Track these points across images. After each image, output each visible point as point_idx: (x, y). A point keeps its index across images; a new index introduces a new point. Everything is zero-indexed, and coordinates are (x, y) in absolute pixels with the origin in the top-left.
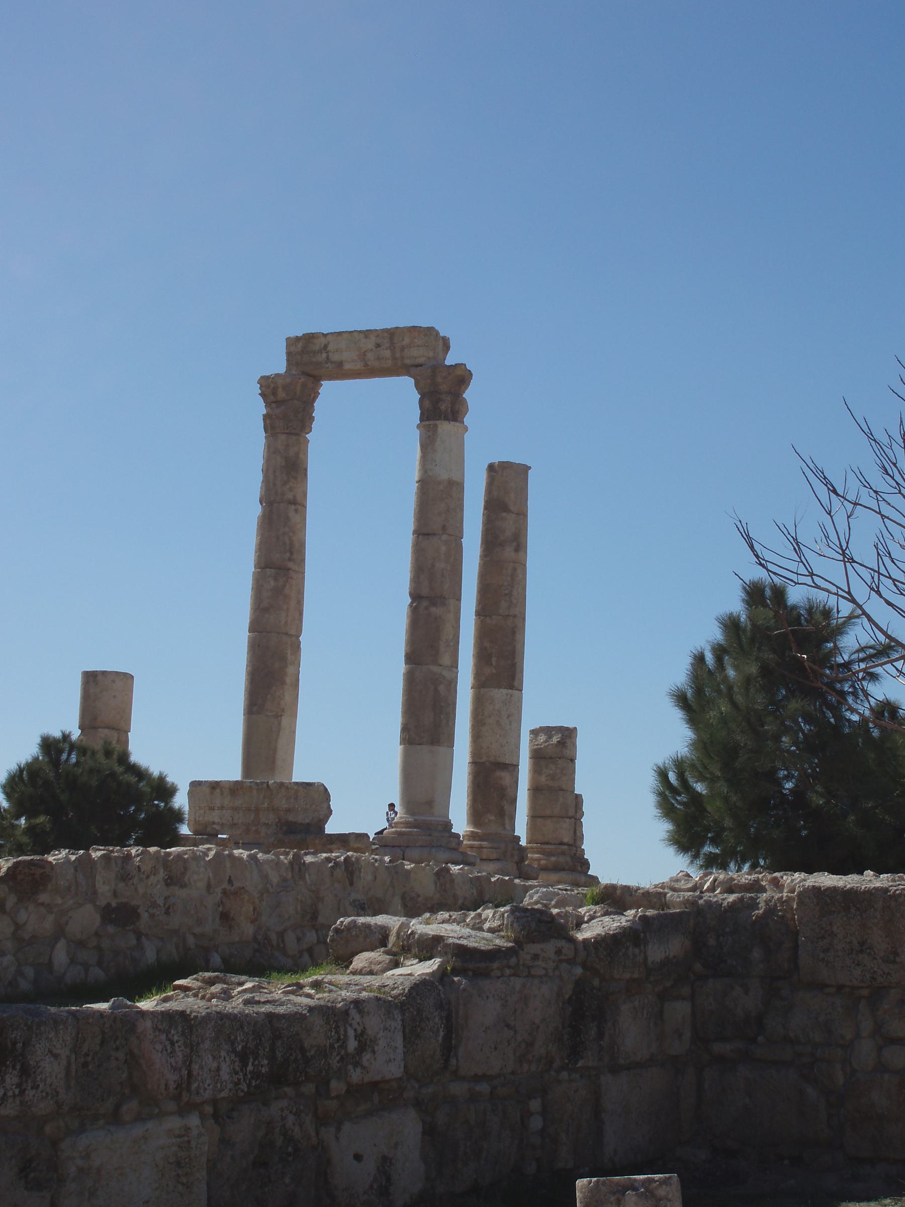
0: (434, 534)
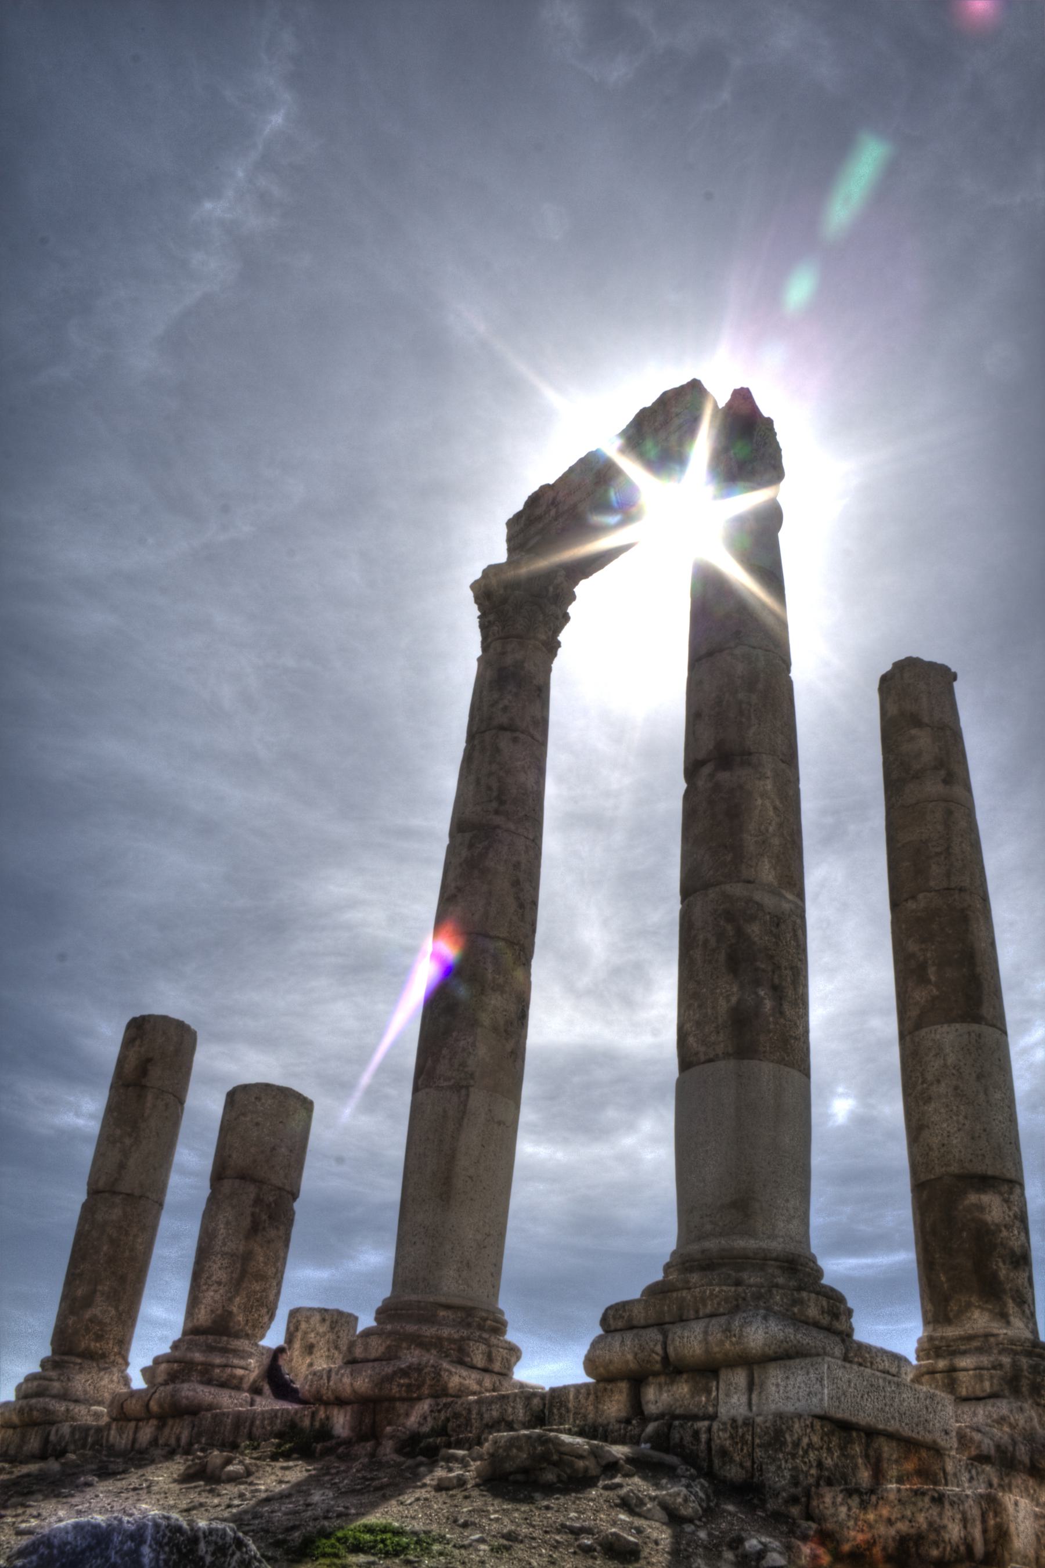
0: (721, 650)
